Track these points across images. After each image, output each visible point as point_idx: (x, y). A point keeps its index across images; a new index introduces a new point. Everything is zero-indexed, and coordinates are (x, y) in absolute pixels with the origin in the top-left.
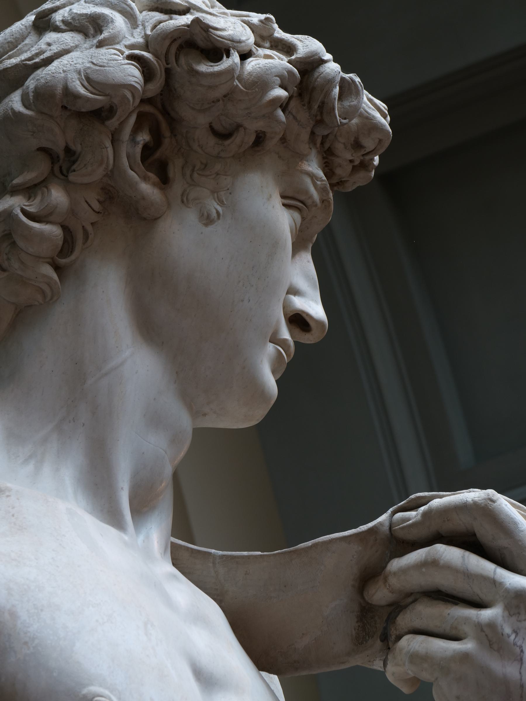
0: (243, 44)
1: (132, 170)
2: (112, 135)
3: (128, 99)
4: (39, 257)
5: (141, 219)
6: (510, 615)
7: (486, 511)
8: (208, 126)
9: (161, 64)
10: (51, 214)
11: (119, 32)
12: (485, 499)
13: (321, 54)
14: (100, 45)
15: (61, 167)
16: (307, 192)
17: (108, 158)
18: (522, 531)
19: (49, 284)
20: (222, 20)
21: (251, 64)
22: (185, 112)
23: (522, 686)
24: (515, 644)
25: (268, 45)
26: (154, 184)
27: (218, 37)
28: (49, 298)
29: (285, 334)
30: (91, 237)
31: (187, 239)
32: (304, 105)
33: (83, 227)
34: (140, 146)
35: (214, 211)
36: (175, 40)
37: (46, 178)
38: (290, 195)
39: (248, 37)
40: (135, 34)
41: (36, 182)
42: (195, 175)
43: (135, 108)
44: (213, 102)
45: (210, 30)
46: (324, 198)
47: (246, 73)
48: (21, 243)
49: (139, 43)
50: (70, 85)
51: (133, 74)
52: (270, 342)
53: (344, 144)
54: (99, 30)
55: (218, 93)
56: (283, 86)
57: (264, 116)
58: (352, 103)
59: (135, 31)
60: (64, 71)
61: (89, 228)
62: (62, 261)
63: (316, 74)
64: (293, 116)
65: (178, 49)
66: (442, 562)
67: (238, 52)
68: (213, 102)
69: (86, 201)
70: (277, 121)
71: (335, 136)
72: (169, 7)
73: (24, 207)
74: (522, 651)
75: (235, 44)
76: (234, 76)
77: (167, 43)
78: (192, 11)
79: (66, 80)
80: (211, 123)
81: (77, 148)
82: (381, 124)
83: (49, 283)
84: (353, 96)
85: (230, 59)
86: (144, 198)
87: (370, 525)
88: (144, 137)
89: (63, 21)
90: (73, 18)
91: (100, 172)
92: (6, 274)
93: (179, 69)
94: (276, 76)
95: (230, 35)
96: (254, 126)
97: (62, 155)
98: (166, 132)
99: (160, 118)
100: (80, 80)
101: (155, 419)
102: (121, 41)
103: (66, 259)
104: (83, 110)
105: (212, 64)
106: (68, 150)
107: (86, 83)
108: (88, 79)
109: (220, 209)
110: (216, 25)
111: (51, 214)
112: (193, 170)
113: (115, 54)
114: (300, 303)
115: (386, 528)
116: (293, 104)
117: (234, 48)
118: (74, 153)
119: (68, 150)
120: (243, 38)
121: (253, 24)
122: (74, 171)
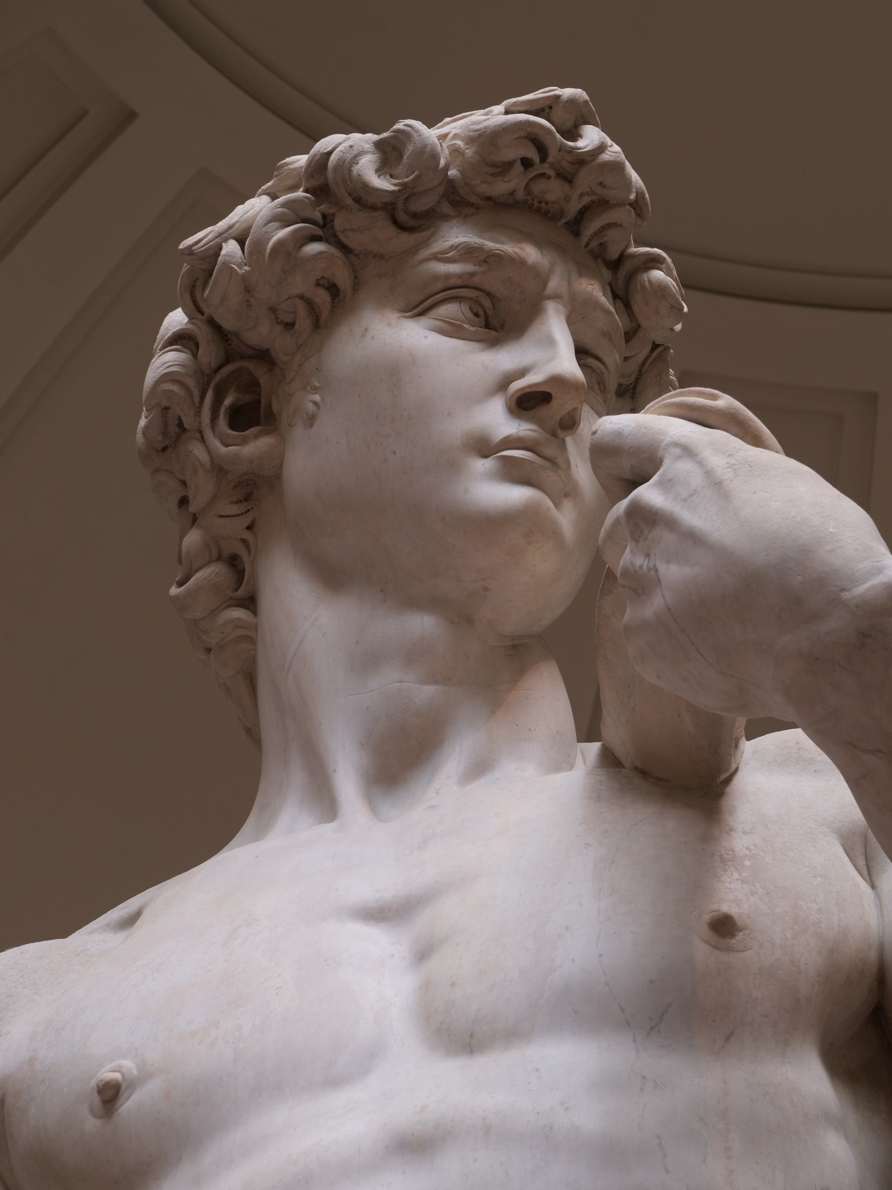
3: (168, 391)
6: (637, 542)
8: (278, 328)
16: (436, 277)
17: (198, 460)
23: (669, 609)
26: (257, 437)
28: (249, 638)
31: (313, 454)
33: (242, 540)
46: (483, 257)
52: (486, 456)
53: (483, 182)
62: (240, 593)
69: (221, 516)
71: (467, 184)
74: (657, 571)
83: (238, 624)
88: (228, 401)
94: (266, 225)
101: (366, 661)
109: (317, 398)
116: (339, 223)
117: (226, 240)
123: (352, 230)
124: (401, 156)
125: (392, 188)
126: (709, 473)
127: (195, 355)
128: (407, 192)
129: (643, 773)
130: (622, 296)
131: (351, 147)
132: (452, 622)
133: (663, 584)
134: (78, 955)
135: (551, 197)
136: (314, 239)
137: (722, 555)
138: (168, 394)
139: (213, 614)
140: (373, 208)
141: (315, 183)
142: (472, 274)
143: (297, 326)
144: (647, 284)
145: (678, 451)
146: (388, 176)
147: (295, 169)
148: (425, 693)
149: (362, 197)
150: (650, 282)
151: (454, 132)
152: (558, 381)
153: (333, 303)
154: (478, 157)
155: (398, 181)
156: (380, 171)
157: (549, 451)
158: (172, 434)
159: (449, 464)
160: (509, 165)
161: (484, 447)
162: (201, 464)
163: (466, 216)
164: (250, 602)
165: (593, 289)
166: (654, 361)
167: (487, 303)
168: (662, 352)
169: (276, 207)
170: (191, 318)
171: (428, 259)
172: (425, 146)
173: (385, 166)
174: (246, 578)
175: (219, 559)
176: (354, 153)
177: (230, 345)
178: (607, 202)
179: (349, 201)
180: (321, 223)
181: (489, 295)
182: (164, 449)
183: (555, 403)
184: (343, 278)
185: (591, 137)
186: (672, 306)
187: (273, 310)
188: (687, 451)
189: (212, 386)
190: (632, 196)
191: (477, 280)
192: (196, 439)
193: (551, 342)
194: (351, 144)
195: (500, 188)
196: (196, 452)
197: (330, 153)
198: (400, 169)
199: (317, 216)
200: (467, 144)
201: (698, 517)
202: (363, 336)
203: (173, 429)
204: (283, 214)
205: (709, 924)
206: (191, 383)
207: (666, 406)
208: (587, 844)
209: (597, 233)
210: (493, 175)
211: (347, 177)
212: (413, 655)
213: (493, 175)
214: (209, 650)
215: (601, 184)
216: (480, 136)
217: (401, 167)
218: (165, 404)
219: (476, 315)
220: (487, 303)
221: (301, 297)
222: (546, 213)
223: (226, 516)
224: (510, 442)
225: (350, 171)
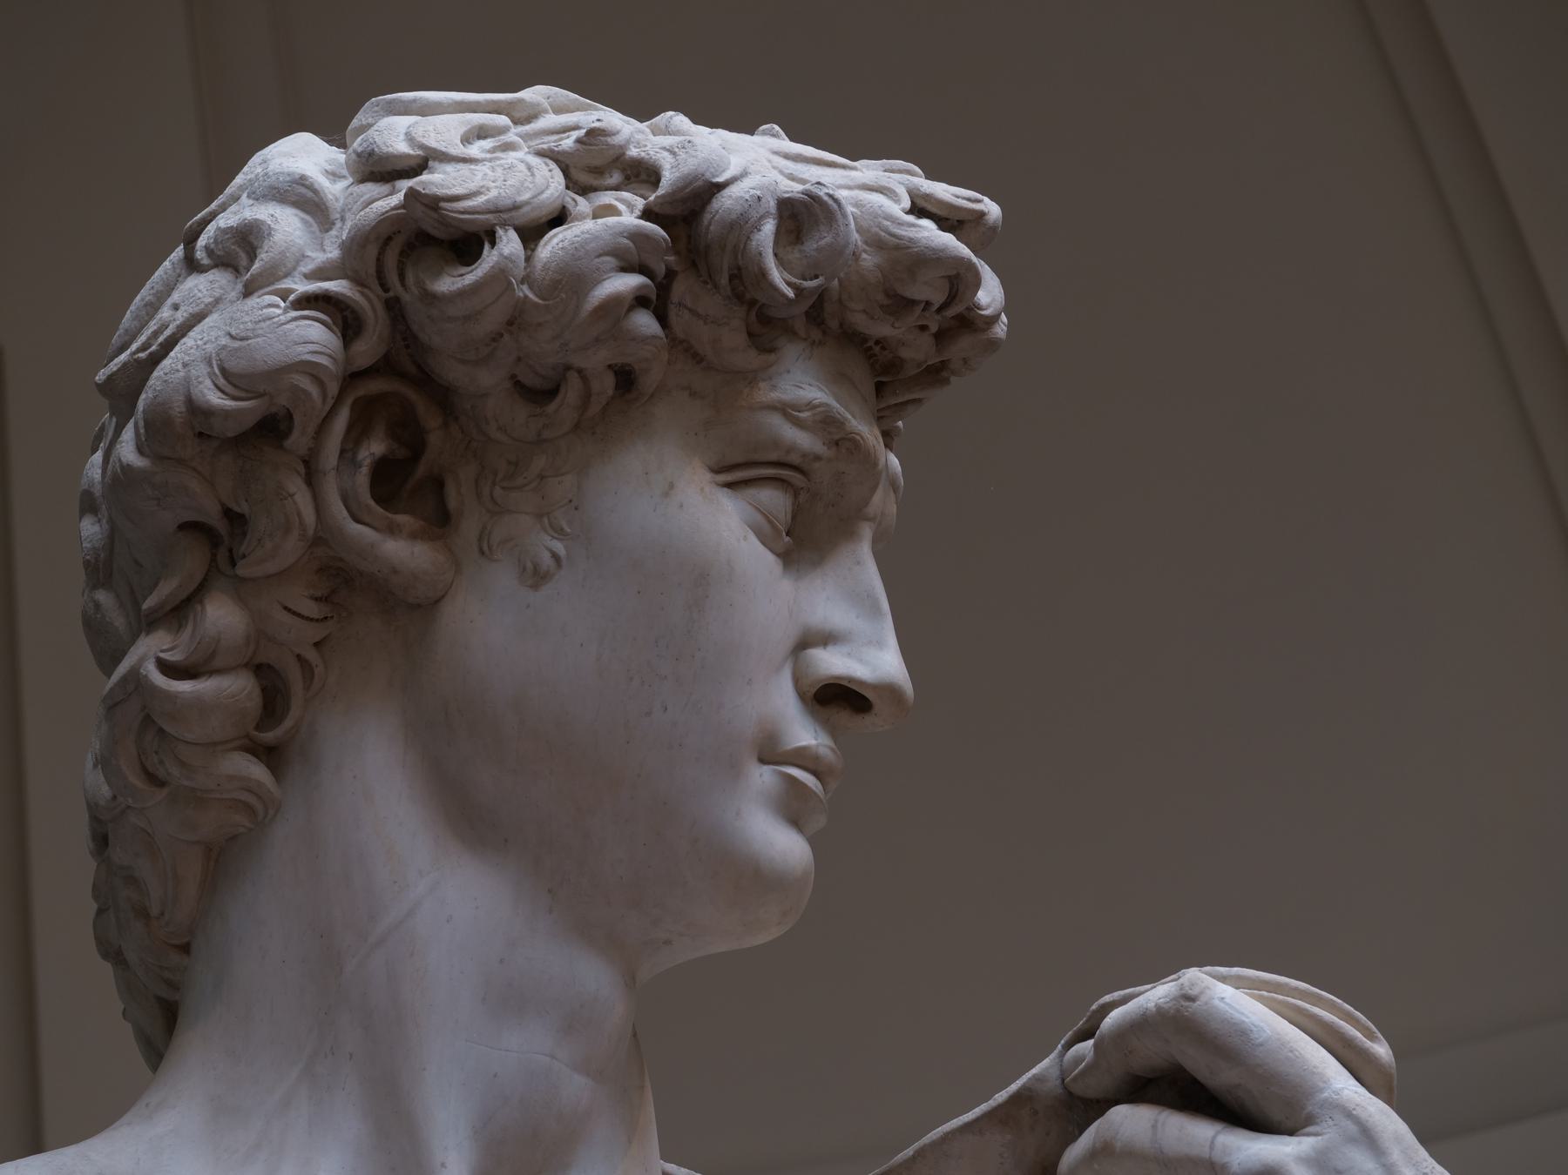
0: (525, 209)
1: (358, 521)
2: (306, 463)
3: (304, 391)
4: (215, 744)
5: (409, 610)
7: (1181, 1020)
9: (371, 295)
10: (213, 655)
11: (282, 253)
12: (1175, 999)
13: (708, 175)
14: (248, 292)
15: (231, 551)
16: (776, 443)
17: (299, 514)
19: (249, 791)
21: (555, 243)
22: (452, 372)
25: (616, 178)
26: (414, 536)
28: (258, 814)
29: (804, 734)
30: (319, 670)
32: (706, 282)
33: (298, 656)
34: (365, 470)
35: (546, 556)
36: (389, 239)
37: (205, 579)
38: (740, 460)
39: (550, 184)
40: (327, 242)
41: (184, 595)
42: (498, 491)
43: (339, 400)
44: (494, 340)
45: (442, 204)
46: (836, 437)
47: (539, 266)
48: (168, 729)
49: (330, 261)
50: (195, 392)
51: (313, 336)
52: (763, 761)
54: (252, 256)
55: (493, 320)
56: (626, 269)
57: (597, 340)
58: (823, 242)
59: (327, 236)
60: (185, 365)
61: (312, 655)
62: (269, 736)
63: (707, 217)
64: (690, 310)
65: (402, 253)
66: (1118, 1145)
67: (517, 230)
68: (494, 340)
69: (286, 608)
70: (634, 339)
71: (840, 301)
72: (389, 168)
73: (162, 655)
75: (505, 216)
76: (510, 283)
77: (373, 251)
78: (431, 163)
79: (187, 380)
80: (513, 377)
81: (243, 508)
84: (822, 228)
85: (495, 252)
86: (395, 571)
87: (1014, 1087)
88: (376, 447)
89: (209, 251)
90: (216, 241)
91: (291, 549)
92: (165, 791)
93: (406, 298)
94: (600, 256)
95: (488, 201)
96: (597, 360)
97: (221, 526)
98: (431, 420)
99: (411, 394)
100: (211, 375)
101: (508, 999)
102: (294, 269)
103: (275, 728)
104: (230, 434)
105: (464, 270)
106: (228, 513)
107: (221, 381)
108: (223, 371)
109: (559, 547)
111: (213, 655)
112: (494, 484)
113: (270, 306)
114: (834, 663)
115: (1053, 1084)
116: (679, 289)
117: (504, 225)
118: (242, 516)
119: (228, 513)
120: (526, 196)
121: (564, 153)
122: (244, 556)
123: (693, 312)
125: (790, 293)
135: (905, 353)
138: (298, 393)
142: (818, 458)
143: (551, 407)
145: (1352, 1128)
148: (576, 1088)
149: (744, 284)
152: (889, 690)
155: (794, 280)
161: (770, 752)
169: (621, 234)
175: (246, 665)
179: (724, 281)
182: (201, 434)
183: (868, 720)
185: (990, 294)
187: (519, 359)
188: (1367, 1137)
189: (349, 401)
195: (883, 329)
196: (298, 498)
197: (720, 187)
198: (794, 255)
199: (661, 270)
200: (866, 243)
202: (666, 494)
206: (333, 388)
210: (881, 307)
213: (881, 307)
214: (154, 780)
216: (897, 248)
221: (580, 371)
223: (294, 613)
224: (801, 757)
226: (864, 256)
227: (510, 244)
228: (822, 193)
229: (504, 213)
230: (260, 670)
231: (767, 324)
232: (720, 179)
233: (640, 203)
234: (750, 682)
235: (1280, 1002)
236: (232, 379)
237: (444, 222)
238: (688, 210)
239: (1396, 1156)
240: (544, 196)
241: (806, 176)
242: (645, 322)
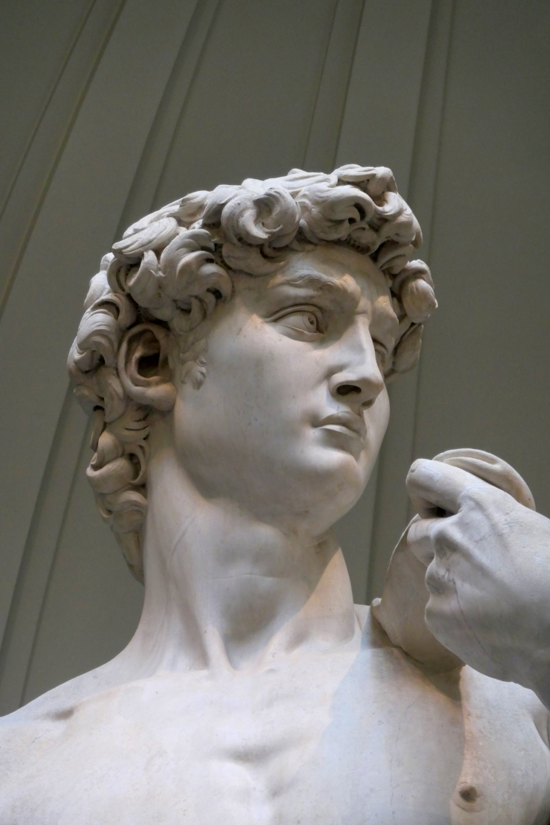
0: (155, 241)
1: (136, 385)
8: (178, 312)
16: (288, 298)
17: (114, 390)
18: (438, 481)
20: (145, 231)
24: (449, 581)
26: (157, 384)
27: (130, 251)
30: (147, 449)
36: (119, 271)
38: (277, 309)
45: (123, 251)
58: (277, 212)
61: (143, 443)
62: (137, 481)
69: (127, 429)
74: (454, 583)
75: (146, 247)
76: (151, 273)
77: (114, 279)
80: (179, 308)
81: (102, 396)
82: (337, 198)
83: (135, 504)
84: (276, 206)
86: (153, 400)
88: (137, 354)
94: (178, 249)
101: (228, 556)
109: (204, 370)
110: (124, 245)
114: (340, 378)
116: (225, 251)
117: (147, 250)
120: (154, 236)
121: (176, 213)
123: (233, 257)
124: (270, 211)
125: (264, 236)
126: (493, 526)
127: (116, 317)
128: (274, 237)
129: (407, 655)
130: (397, 295)
131: (239, 204)
132: (285, 534)
133: (459, 594)
134: (34, 742)
136: (210, 261)
137: (501, 586)
139: (117, 492)
140: (250, 245)
141: (210, 221)
142: (312, 297)
144: (415, 290)
145: (472, 503)
146: (261, 225)
147: (195, 203)
148: (266, 583)
149: (244, 240)
150: (417, 289)
151: (304, 191)
152: (366, 381)
153: (217, 302)
154: (321, 215)
156: (256, 222)
157: (356, 426)
158: (96, 364)
159: (291, 432)
160: (341, 222)
161: (316, 421)
162: (117, 394)
163: (309, 251)
164: (142, 488)
165: (385, 303)
166: (411, 333)
167: (319, 315)
168: (417, 327)
169: (185, 238)
170: (114, 291)
171: (283, 284)
172: (288, 209)
173: (259, 218)
174: (141, 473)
175: (122, 455)
176: (241, 209)
177: (139, 311)
178: (398, 243)
179: (235, 241)
180: (214, 250)
181: (320, 308)
182: (86, 372)
184: (226, 289)
186: (430, 306)
188: (479, 506)
190: (414, 239)
191: (314, 301)
192: (114, 375)
193: (360, 349)
194: (239, 202)
195: (334, 236)
197: (224, 205)
198: (269, 221)
199: (212, 246)
200: (313, 204)
201: (485, 556)
203: (96, 361)
204: (190, 243)
205: (460, 792)
206: (113, 337)
207: (461, 461)
208: (380, 722)
209: (388, 261)
210: (329, 227)
211: (235, 225)
212: (259, 556)
215: (397, 234)
216: (324, 202)
217: (270, 220)
218: (94, 349)
219: (312, 323)
220: (319, 315)
221: (196, 297)
222: (358, 247)
225: (238, 221)
226: (313, 210)
227: (149, 257)
228: (272, 192)
229: (146, 246)
230: (132, 457)
231: (273, 251)
232: (223, 202)
233: (201, 221)
234: (294, 397)
235: (454, 460)
236: (82, 346)
237: (128, 257)
238: (215, 219)
239: (491, 509)
240: (163, 233)
241: (295, 186)
242: (210, 269)
